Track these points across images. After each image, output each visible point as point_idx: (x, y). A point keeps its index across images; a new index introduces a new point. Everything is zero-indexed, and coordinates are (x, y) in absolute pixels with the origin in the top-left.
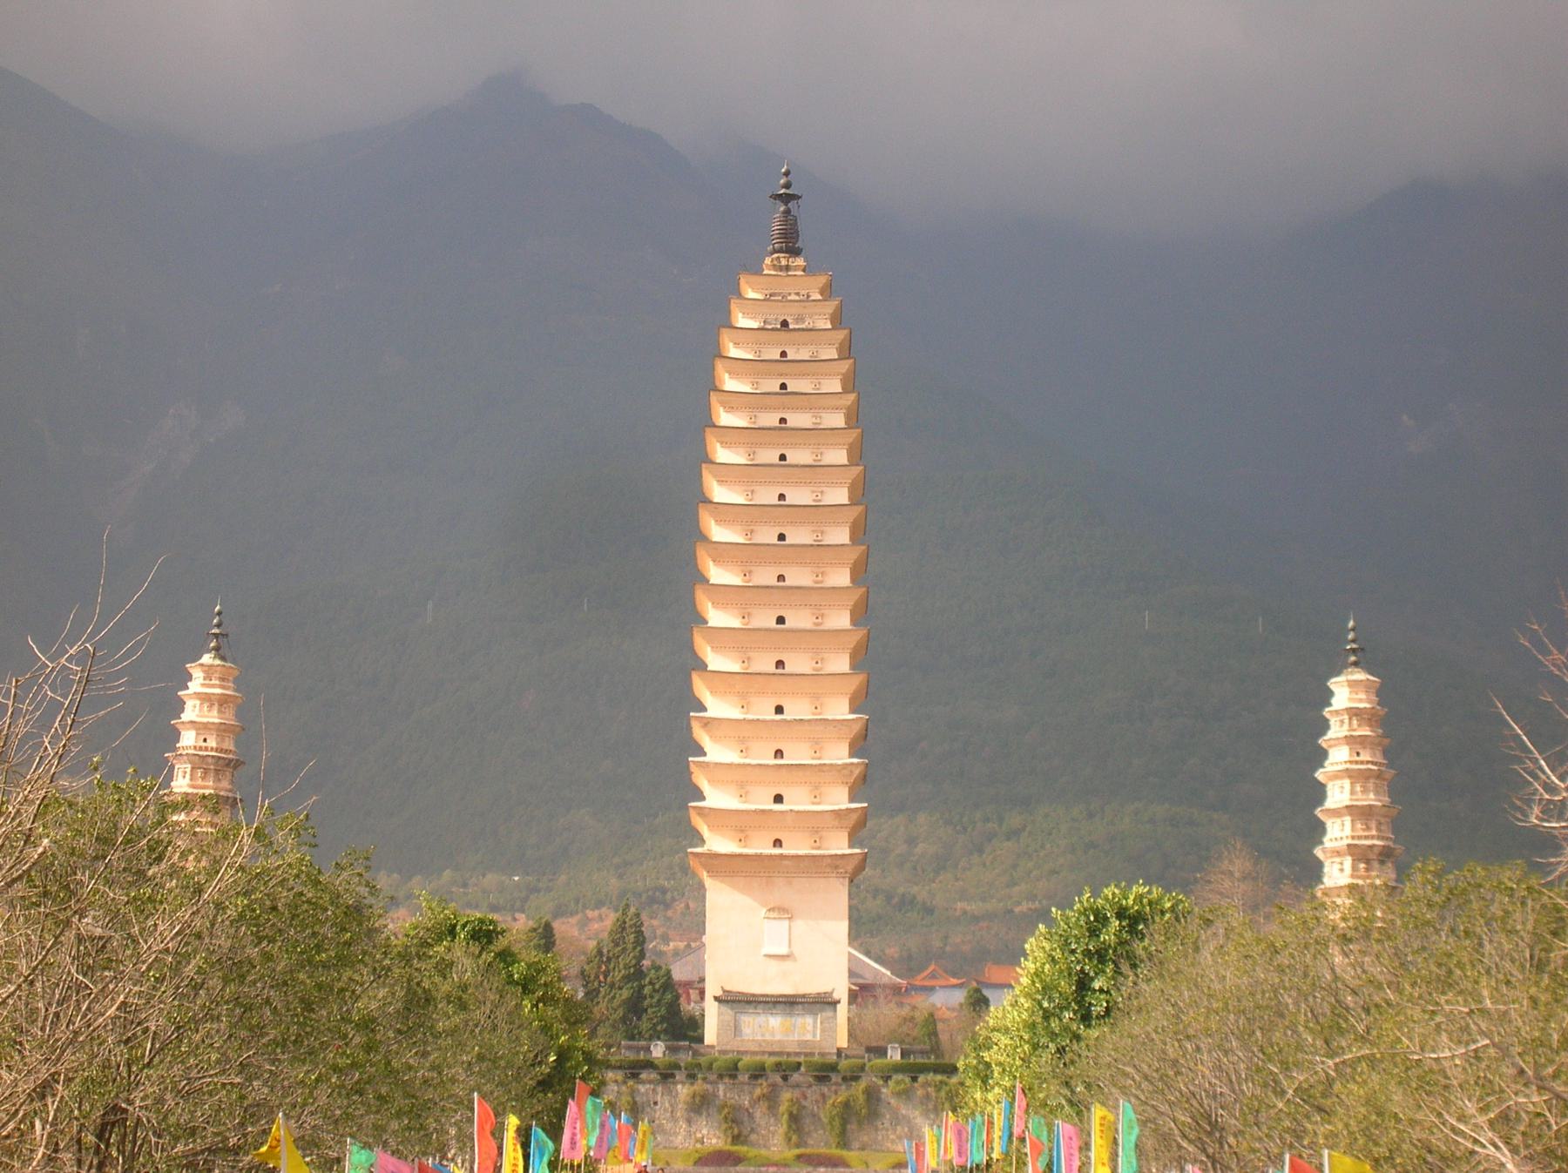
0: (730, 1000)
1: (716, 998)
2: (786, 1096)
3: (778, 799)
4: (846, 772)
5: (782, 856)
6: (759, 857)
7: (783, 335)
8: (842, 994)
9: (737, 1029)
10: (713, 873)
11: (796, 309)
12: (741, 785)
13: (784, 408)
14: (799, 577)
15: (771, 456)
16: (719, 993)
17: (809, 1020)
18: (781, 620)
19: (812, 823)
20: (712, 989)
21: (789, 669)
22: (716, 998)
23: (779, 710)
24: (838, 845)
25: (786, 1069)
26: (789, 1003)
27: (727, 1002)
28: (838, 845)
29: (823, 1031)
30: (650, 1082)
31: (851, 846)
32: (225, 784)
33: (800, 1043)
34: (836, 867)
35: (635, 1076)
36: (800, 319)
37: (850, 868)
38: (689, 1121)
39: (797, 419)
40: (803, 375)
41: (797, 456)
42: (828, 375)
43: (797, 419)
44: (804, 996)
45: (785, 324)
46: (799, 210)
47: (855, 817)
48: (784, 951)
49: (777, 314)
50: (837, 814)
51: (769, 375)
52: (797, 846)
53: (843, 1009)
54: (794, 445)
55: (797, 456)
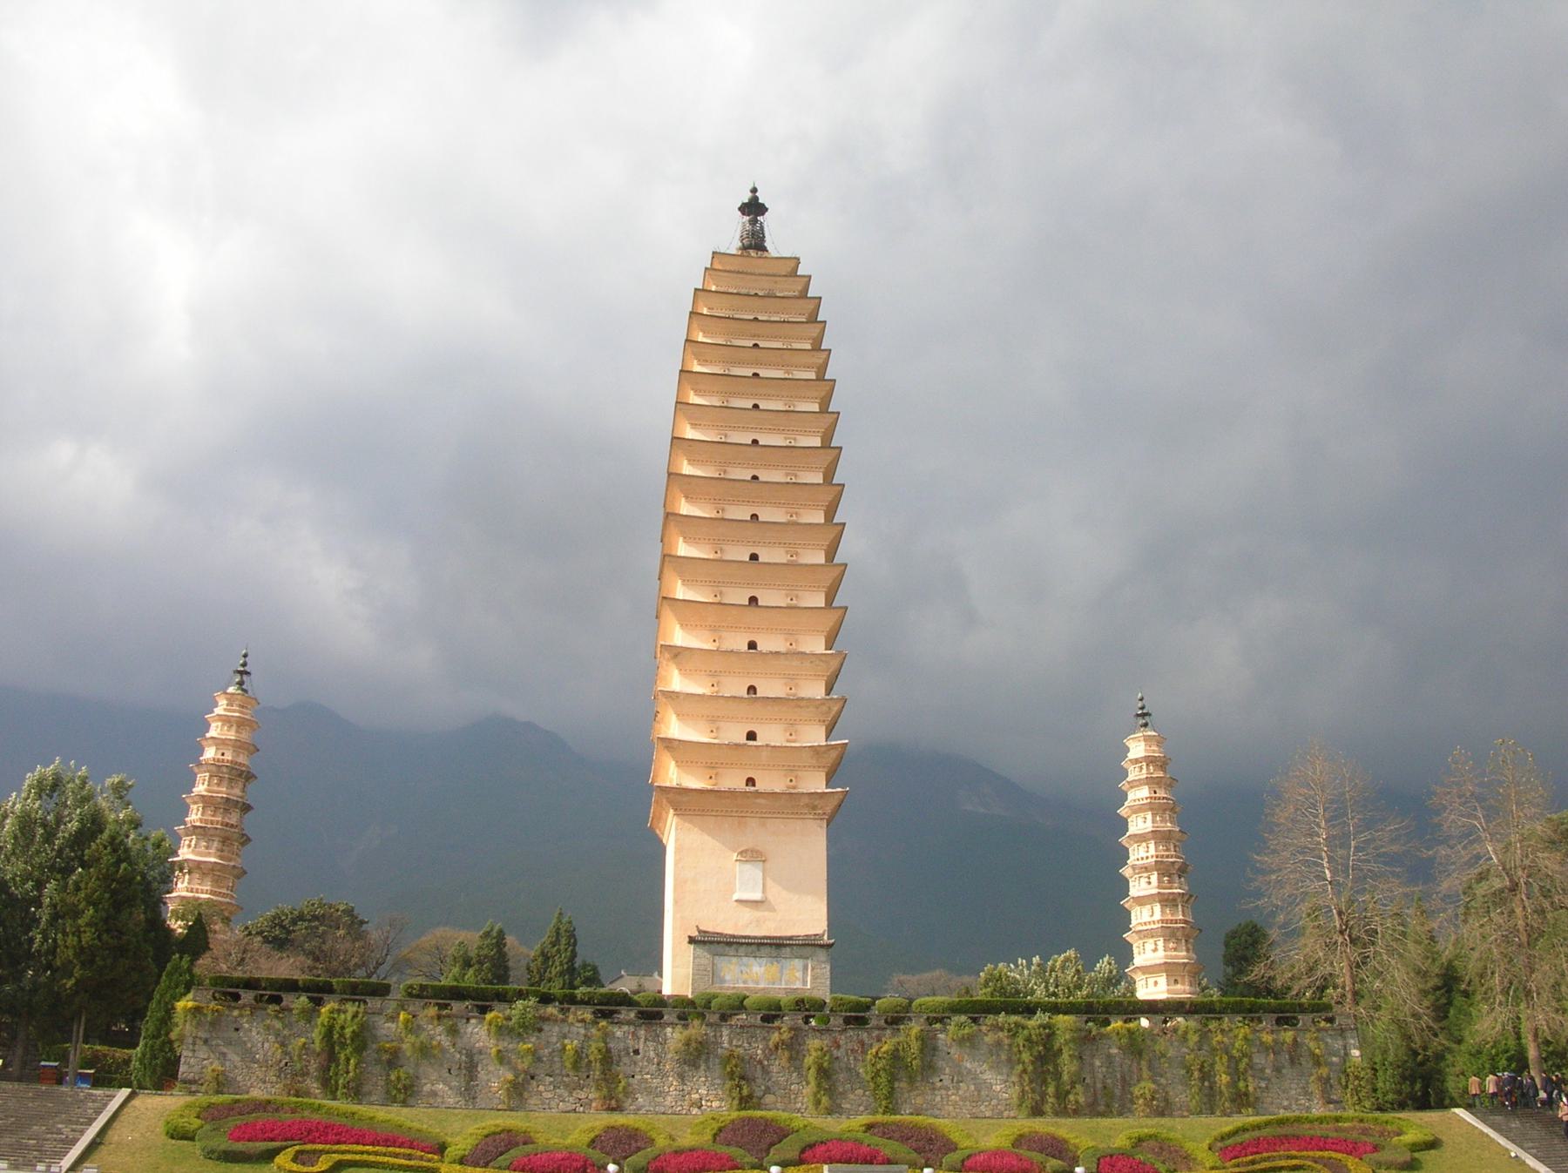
0: (704, 941)
1: (692, 940)
2: (814, 1044)
3: (751, 736)
4: (824, 708)
5: (758, 794)
6: (732, 793)
9: (714, 974)
10: (680, 811)
12: (713, 720)
16: (695, 934)
17: (798, 963)
19: (786, 757)
22: (692, 940)
24: (816, 783)
26: (776, 946)
27: (704, 943)
28: (816, 783)
29: (814, 978)
30: (629, 1023)
32: (237, 791)
33: (788, 991)
34: (814, 808)
35: (606, 1015)
37: (828, 810)
38: (682, 1077)
40: (775, 337)
42: (800, 338)
44: (790, 938)
46: (767, 220)
47: (834, 754)
48: (757, 896)
50: (815, 750)
51: (742, 335)
52: (770, 782)
54: (768, 397)
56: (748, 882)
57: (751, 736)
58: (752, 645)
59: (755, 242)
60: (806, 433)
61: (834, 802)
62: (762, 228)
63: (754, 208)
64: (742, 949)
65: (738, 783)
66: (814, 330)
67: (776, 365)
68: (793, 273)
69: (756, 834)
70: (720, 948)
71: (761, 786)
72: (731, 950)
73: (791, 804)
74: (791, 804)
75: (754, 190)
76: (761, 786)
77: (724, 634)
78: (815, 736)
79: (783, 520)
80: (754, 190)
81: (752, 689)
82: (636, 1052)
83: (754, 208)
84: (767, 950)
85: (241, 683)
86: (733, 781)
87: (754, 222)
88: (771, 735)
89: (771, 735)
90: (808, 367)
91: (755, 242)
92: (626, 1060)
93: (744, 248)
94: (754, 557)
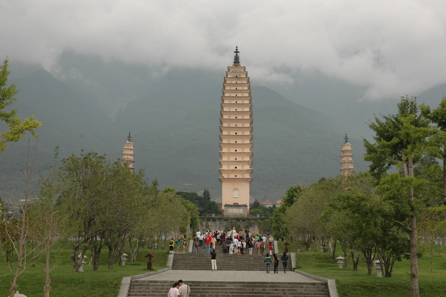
0: (226, 206)
3: (236, 168)
5: (236, 179)
6: (232, 179)
7: (236, 79)
8: (248, 205)
11: (239, 74)
13: (237, 93)
14: (239, 125)
15: (234, 102)
18: (236, 133)
20: (223, 204)
21: (238, 143)
23: (236, 151)
24: (247, 176)
25: (238, 220)
28: (247, 176)
31: (250, 176)
36: (239, 76)
39: (239, 95)
40: (240, 86)
41: (239, 102)
42: (245, 86)
43: (239, 95)
45: (237, 76)
49: (235, 75)
50: (247, 170)
51: (233, 86)
52: (239, 176)
53: (248, 207)
54: (238, 100)
55: (239, 102)
56: (236, 194)
57: (236, 168)
59: (237, 61)
60: (246, 107)
61: (250, 180)
63: (237, 52)
65: (234, 177)
66: (248, 84)
68: (245, 69)
69: (237, 185)
73: (243, 180)
74: (243, 180)
75: (237, 47)
76: (237, 177)
78: (247, 167)
79: (241, 126)
80: (237, 47)
81: (236, 159)
83: (237, 52)
85: (129, 140)
86: (232, 176)
87: (237, 55)
88: (239, 167)
90: (247, 93)
91: (237, 61)
93: (234, 62)
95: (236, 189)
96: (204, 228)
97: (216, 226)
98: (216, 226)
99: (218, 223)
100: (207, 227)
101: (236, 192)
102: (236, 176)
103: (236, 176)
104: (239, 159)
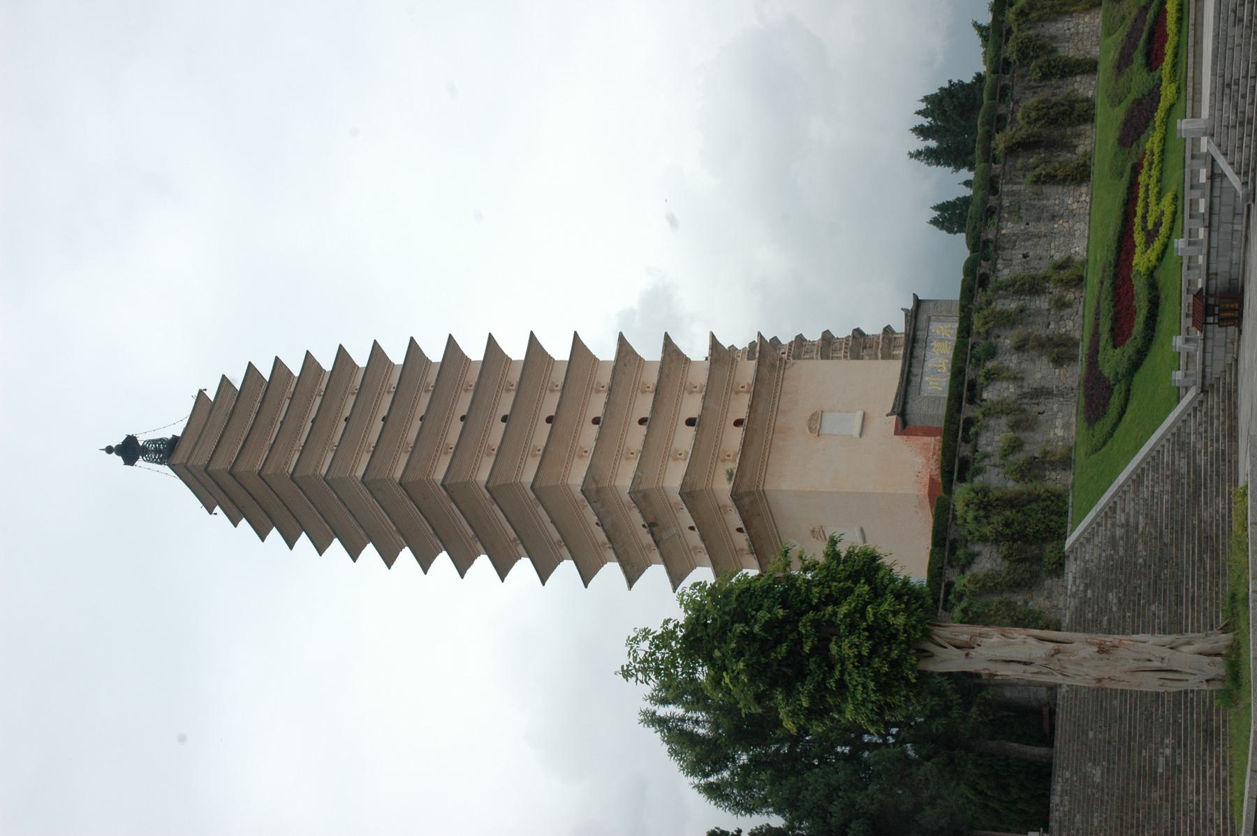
34: (773, 366)
38: (1053, 218)
48: (859, 415)
52: (740, 407)
58: (596, 421)
59: (165, 451)
62: (154, 442)
63: (130, 450)
64: (914, 370)
67: (310, 400)
70: (912, 390)
71: (743, 414)
72: (915, 380)
75: (109, 450)
77: (581, 443)
80: (109, 450)
82: (1025, 256)
83: (130, 450)
84: (918, 352)
86: (734, 438)
89: (692, 406)
91: (165, 451)
92: (1034, 263)
94: (504, 419)
95: (815, 422)
96: (1042, 303)
97: (1029, 236)
98: (1029, 236)
99: (1008, 228)
100: (1033, 287)
101: (831, 423)
102: (738, 423)
103: (738, 423)
104: (644, 406)
